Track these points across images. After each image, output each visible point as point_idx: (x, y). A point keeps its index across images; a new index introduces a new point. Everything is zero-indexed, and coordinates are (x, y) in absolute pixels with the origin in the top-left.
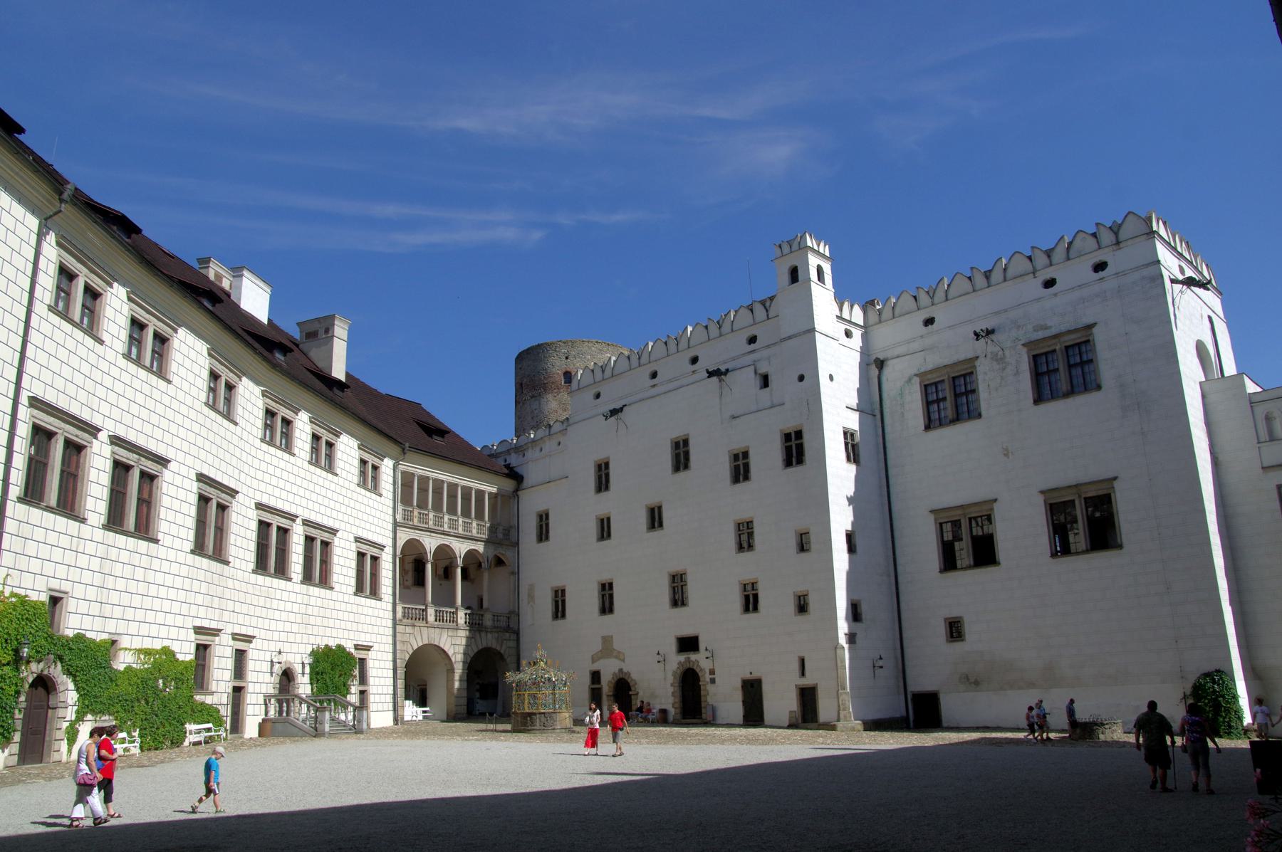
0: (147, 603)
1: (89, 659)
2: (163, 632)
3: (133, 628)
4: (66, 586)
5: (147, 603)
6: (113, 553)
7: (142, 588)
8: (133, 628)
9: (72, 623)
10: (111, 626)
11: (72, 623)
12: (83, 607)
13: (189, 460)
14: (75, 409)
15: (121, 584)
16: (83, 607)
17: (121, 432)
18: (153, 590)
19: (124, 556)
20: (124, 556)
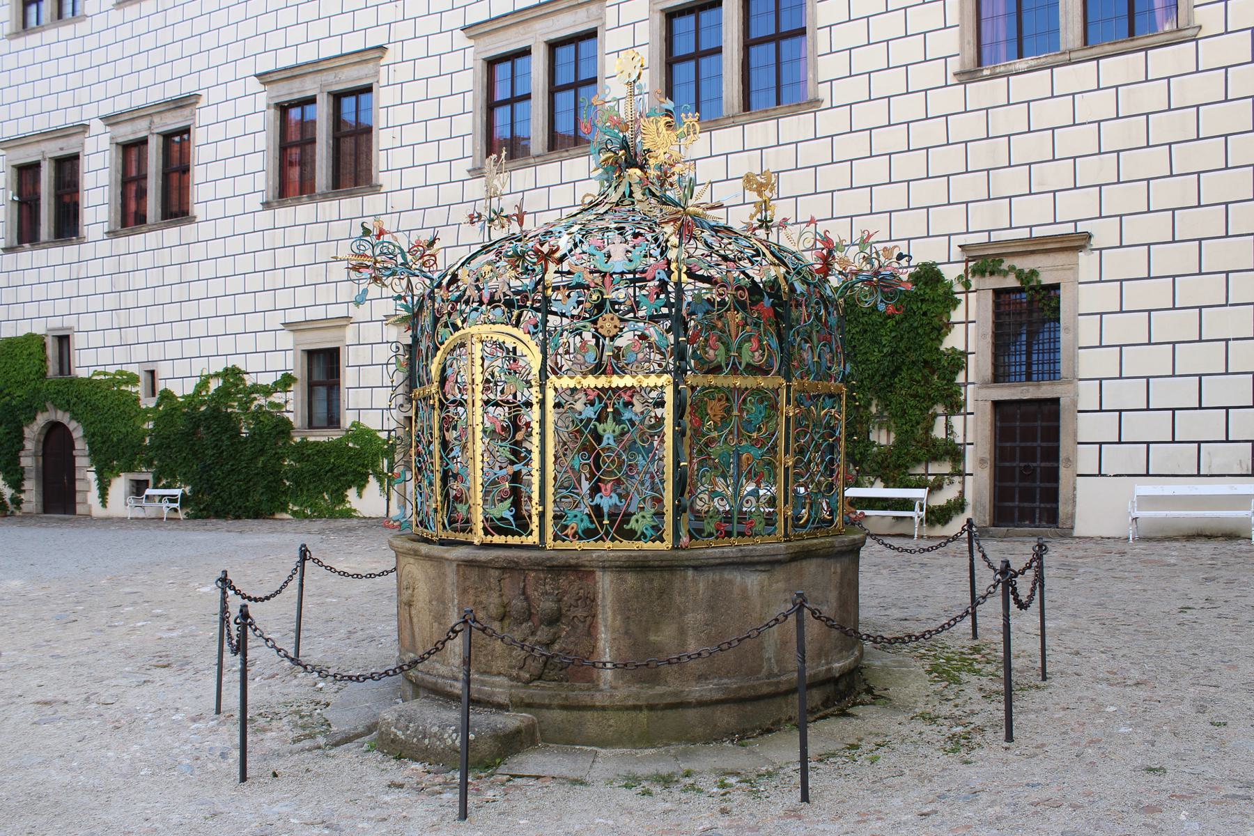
0: (190, 310)
1: (104, 404)
2: (226, 345)
3: (173, 350)
4: (69, 322)
5: (190, 310)
6: (128, 263)
7: (179, 293)
8: (173, 350)
9: (85, 364)
10: (140, 354)
11: (85, 364)
12: (96, 339)
13: (227, 73)
14: (41, 124)
15: (146, 297)
16: (96, 339)
17: (107, 109)
18: (198, 290)
19: (145, 260)
20: (145, 260)
